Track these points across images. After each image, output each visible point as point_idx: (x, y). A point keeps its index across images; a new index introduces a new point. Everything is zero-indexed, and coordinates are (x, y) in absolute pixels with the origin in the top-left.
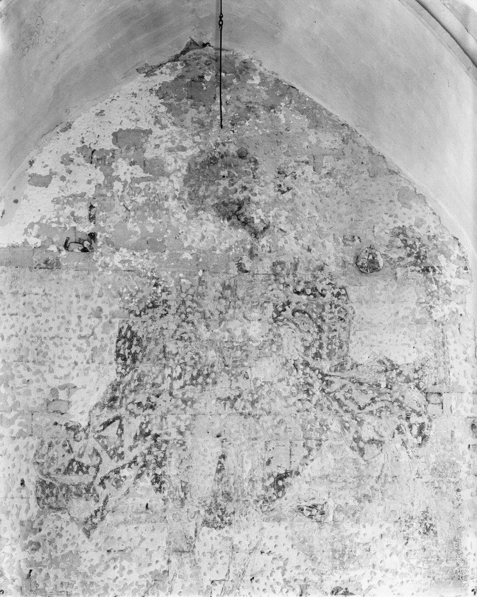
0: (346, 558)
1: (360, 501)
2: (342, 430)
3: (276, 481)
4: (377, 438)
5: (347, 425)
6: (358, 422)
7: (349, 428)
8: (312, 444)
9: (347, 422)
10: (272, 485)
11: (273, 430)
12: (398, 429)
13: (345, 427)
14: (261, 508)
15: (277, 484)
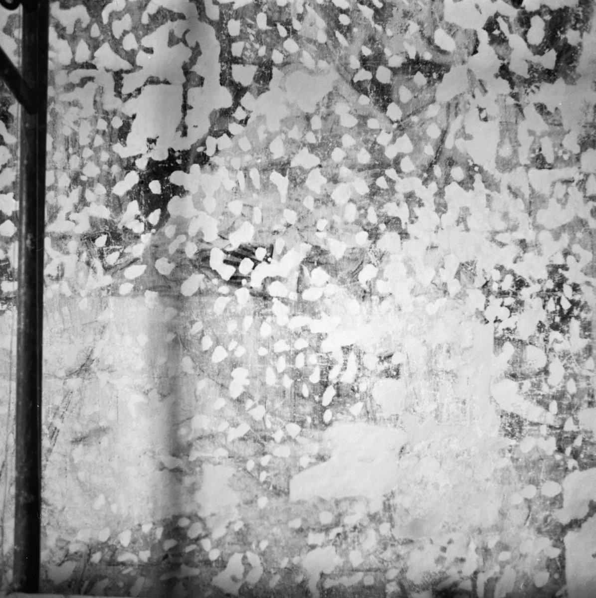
0: (330, 394)
1: (374, 235)
2: (330, 34)
3: (144, 182)
4: (428, 56)
5: (344, 20)
6: (377, 11)
7: (349, 28)
8: (244, 74)
9: (345, 12)
10: (133, 194)
11: (138, 39)
12: (491, 25)
13: (339, 27)
14: (102, 257)
15: (148, 191)
